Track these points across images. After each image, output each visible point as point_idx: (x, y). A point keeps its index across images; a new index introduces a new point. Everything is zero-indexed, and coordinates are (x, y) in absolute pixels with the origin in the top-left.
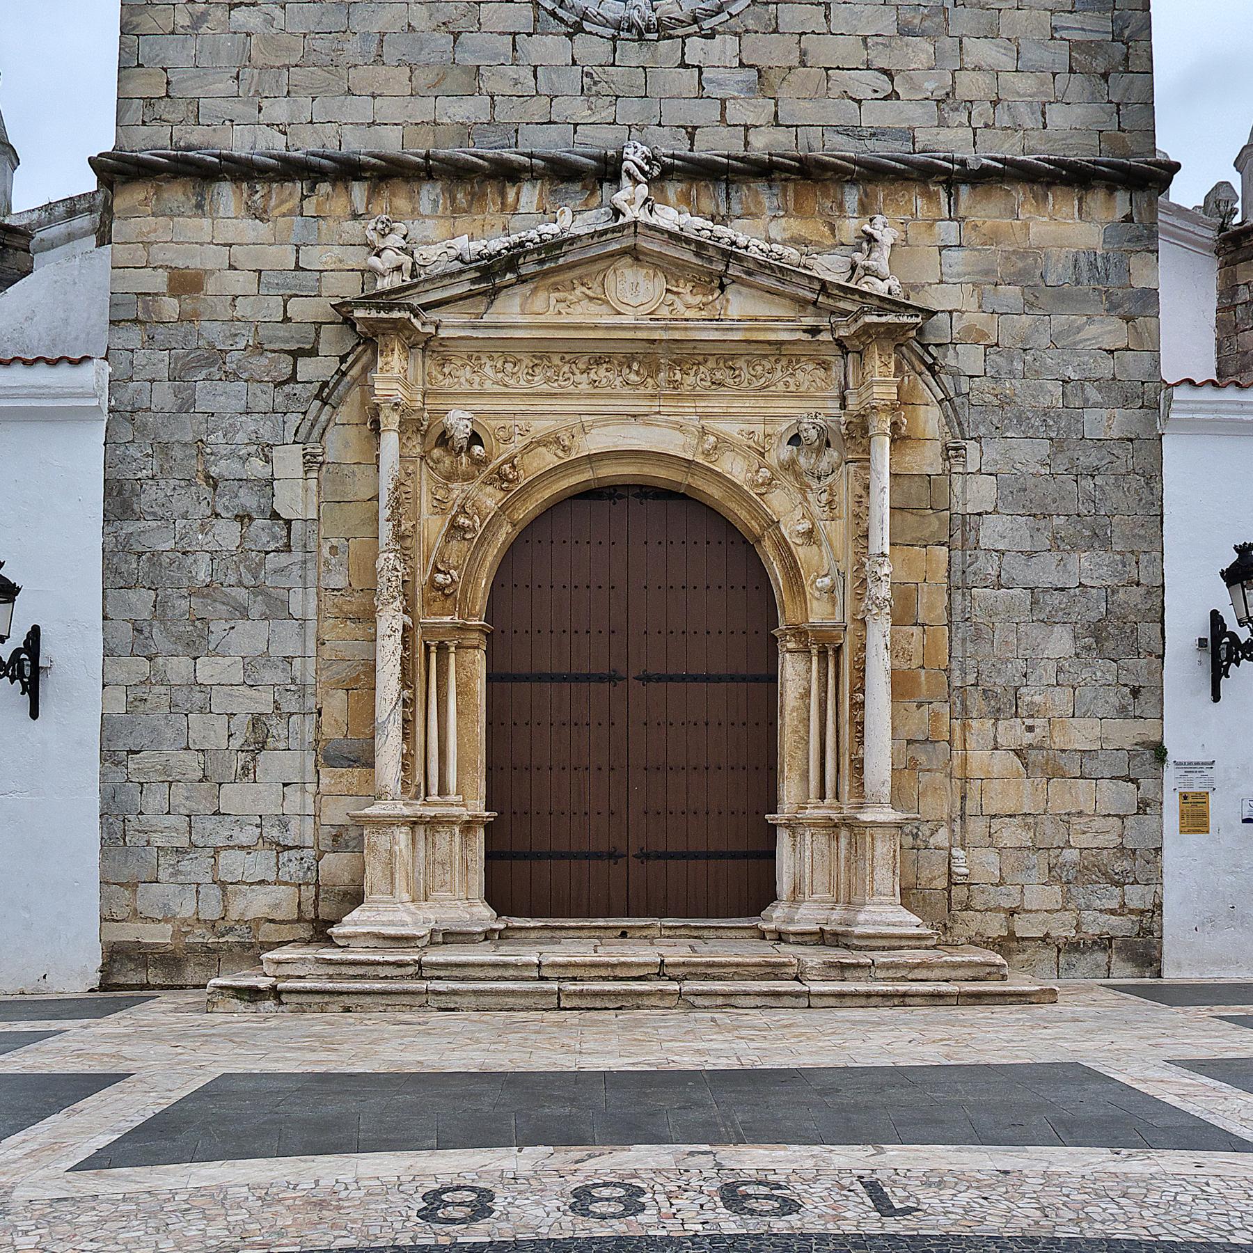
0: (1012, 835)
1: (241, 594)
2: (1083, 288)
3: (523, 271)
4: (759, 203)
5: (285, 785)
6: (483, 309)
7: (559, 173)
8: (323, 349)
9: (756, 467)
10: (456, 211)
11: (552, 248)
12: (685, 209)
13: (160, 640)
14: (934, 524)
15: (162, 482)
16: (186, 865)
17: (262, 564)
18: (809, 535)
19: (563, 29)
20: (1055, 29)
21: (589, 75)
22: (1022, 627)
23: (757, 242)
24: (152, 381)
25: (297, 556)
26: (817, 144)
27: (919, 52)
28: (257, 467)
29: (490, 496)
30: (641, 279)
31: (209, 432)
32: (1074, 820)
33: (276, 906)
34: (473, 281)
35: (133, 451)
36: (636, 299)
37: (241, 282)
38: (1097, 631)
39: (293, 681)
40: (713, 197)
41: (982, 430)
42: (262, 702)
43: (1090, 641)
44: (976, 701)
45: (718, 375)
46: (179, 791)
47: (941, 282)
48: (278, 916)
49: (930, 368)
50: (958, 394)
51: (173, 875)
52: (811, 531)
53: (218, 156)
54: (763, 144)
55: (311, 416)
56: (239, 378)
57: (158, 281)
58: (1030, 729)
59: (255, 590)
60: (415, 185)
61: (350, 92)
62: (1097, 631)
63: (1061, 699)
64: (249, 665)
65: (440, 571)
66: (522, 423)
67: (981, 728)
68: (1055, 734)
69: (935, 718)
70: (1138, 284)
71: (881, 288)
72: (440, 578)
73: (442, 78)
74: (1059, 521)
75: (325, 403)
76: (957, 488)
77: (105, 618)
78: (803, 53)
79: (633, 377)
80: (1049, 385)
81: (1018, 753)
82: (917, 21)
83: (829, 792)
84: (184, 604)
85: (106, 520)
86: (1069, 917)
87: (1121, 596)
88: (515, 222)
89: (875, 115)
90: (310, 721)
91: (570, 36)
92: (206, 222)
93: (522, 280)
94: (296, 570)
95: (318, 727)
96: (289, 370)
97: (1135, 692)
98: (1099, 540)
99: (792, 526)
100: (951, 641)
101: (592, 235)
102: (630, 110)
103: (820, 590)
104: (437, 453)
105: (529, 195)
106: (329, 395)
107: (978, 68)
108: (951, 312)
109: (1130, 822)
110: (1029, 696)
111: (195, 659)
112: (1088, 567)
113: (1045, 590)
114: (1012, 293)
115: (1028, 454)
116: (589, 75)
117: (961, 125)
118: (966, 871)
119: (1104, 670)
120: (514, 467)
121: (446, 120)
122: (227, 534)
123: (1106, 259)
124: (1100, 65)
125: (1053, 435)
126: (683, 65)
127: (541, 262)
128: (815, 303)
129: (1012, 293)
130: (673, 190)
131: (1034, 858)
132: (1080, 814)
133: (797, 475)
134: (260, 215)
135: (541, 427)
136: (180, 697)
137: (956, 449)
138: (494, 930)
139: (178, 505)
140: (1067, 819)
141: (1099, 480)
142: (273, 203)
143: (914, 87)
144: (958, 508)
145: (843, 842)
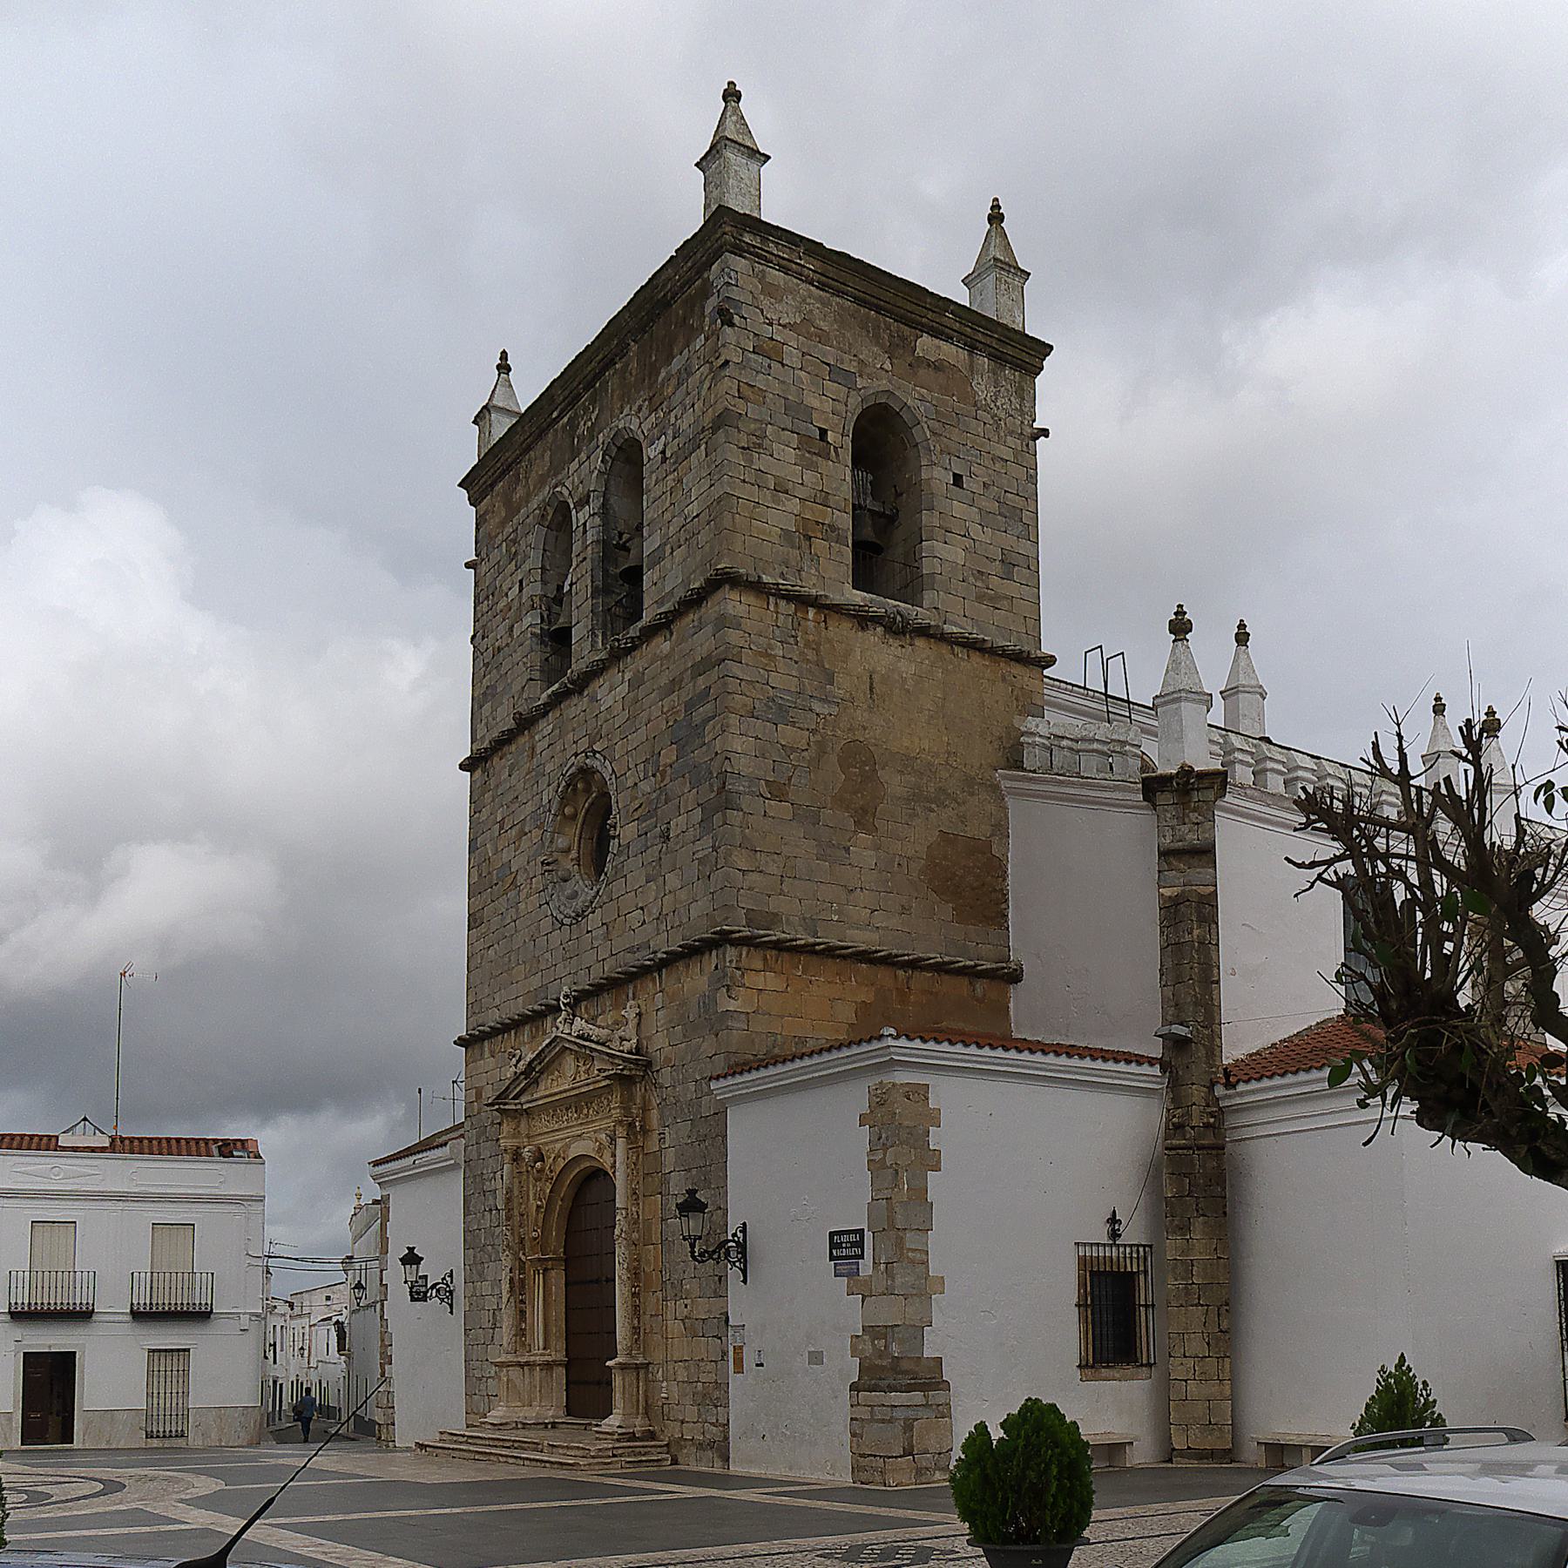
0: (682, 1375)
93: (541, 1072)
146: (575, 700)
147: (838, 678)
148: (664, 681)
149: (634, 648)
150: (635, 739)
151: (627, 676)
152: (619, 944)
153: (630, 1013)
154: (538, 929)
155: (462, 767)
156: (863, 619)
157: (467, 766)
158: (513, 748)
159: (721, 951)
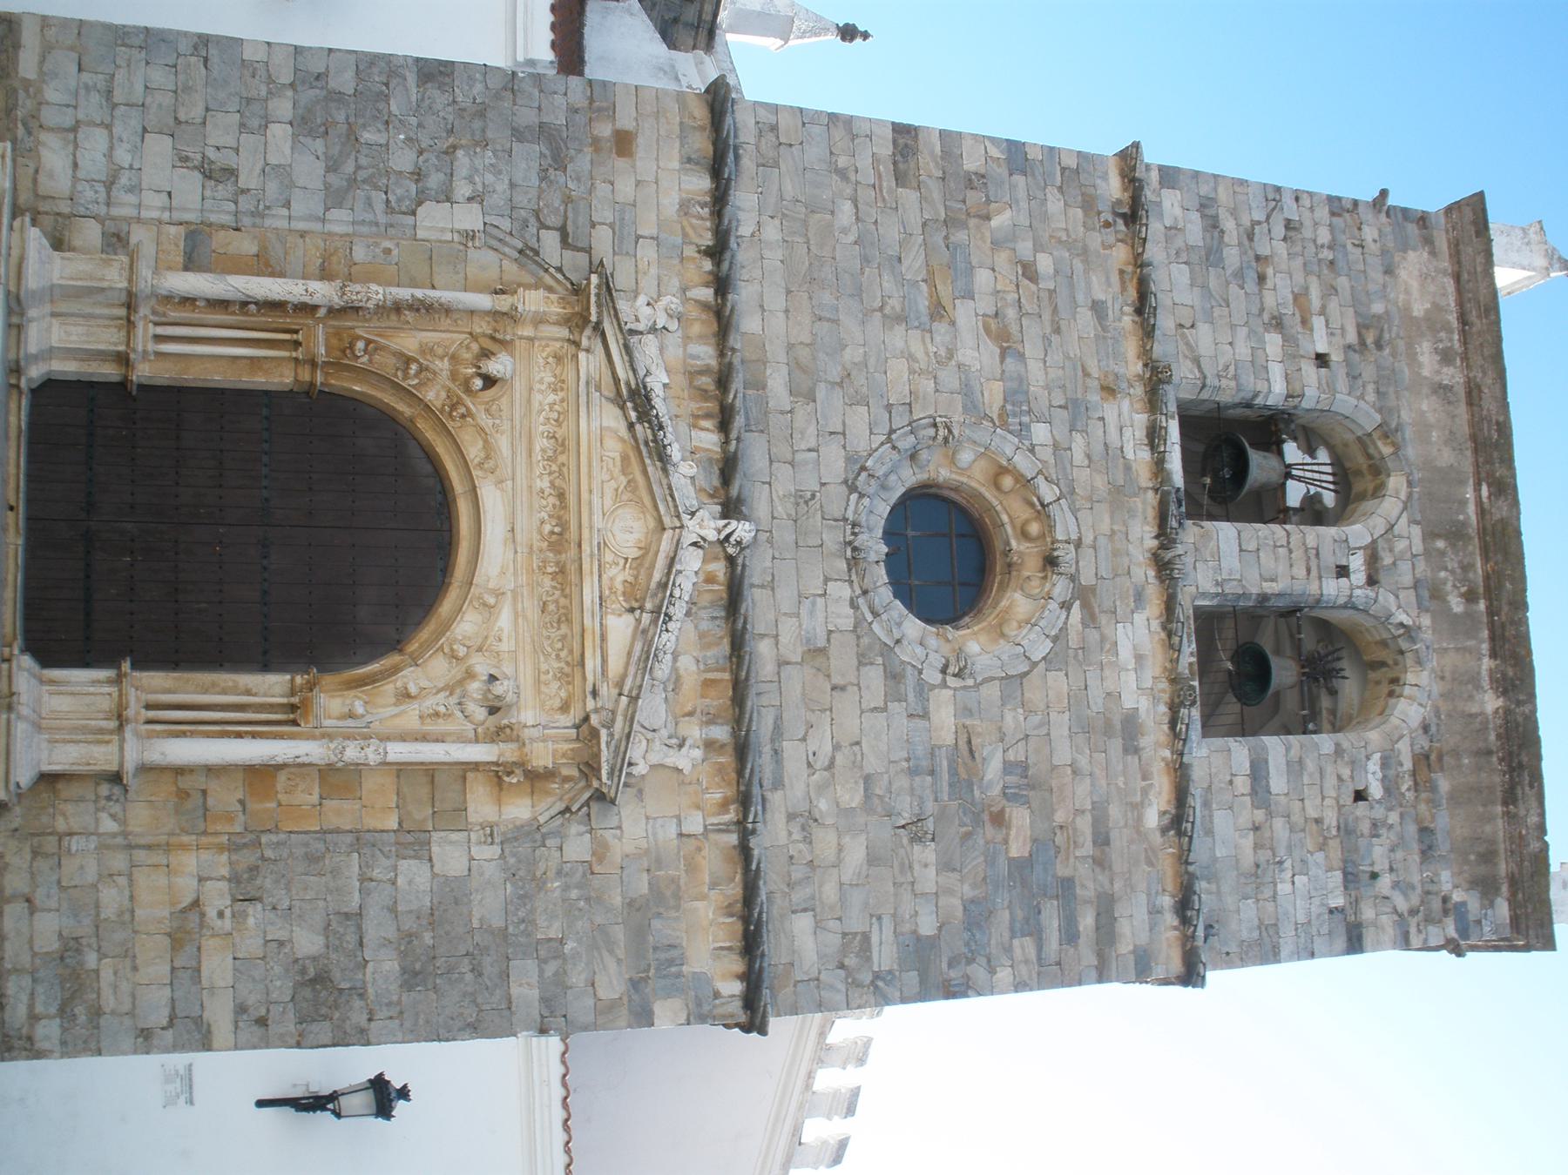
0: (111, 899)
1: (349, 167)
2: (651, 955)
3: (638, 427)
4: (707, 646)
5: (169, 194)
6: (606, 393)
7: (728, 467)
8: (568, 254)
9: (468, 643)
10: (692, 374)
11: (662, 457)
12: (702, 577)
13: (309, 95)
14: (422, 813)
15: (450, 109)
16: (95, 98)
17: (376, 188)
18: (406, 696)
19: (851, 476)
20: (879, 918)
21: (813, 496)
22: (321, 904)
23: (673, 639)
24: (539, 108)
25: (382, 219)
26: (764, 700)
27: (851, 796)
28: (462, 190)
29: (438, 395)
30: (636, 536)
31: (494, 152)
32: (128, 962)
33: (51, 176)
34: (628, 384)
35: (479, 87)
36: (619, 530)
37: (625, 189)
38: (321, 980)
39: (268, 208)
40: (713, 604)
41: (512, 861)
42: (248, 179)
43: (312, 972)
44: (247, 858)
45: (552, 607)
46: (168, 100)
47: (647, 818)
48: (42, 178)
49: (568, 809)
50: (544, 837)
51: (87, 88)
52: (408, 696)
53: (729, 180)
54: (763, 651)
55: (508, 239)
56: (542, 180)
57: (625, 121)
58: (221, 915)
59: (352, 182)
60: (713, 341)
61: (789, 292)
62: (321, 980)
63: (251, 945)
64: (283, 172)
65: (367, 346)
66: (506, 426)
67: (221, 864)
68: (217, 940)
69: (230, 818)
71: (636, 752)
72: (360, 345)
73: (804, 370)
74: (428, 938)
75: (521, 252)
76: (454, 836)
77: (330, 50)
78: (843, 688)
79: (547, 528)
80: (557, 925)
81: (196, 903)
82: (878, 791)
83: (152, 714)
84: (341, 117)
85: (418, 60)
86: (25, 960)
87: (357, 1003)
88: (683, 427)
89: (793, 752)
90: (227, 219)
91: (845, 482)
92: (676, 165)
93: (631, 426)
94: (369, 217)
95: (223, 227)
96: (549, 223)
97: (262, 1022)
98: (412, 978)
99: (411, 678)
100: (306, 833)
101: (670, 488)
102: (785, 535)
103: (352, 704)
104: (475, 347)
105: (709, 439)
106: (527, 256)
107: (840, 849)
108: (620, 828)
109: (127, 1021)
110: (254, 913)
111: (291, 123)
112: (384, 968)
113: (359, 927)
114: (642, 886)
115: (488, 907)
116: (813, 496)
117: (790, 834)
118: (74, 848)
119: (282, 988)
120: (463, 416)
121: (769, 372)
122: (403, 160)
123: (679, 975)
124: (851, 961)
125: (511, 929)
126: (827, 580)
127: (646, 444)
128: (620, 694)
129: (642, 886)
130: (719, 568)
131: (87, 921)
132: (135, 969)
133: (461, 682)
134: (684, 207)
135: (503, 443)
136: (256, 107)
137: (491, 835)
138: (19, 379)
139: (430, 121)
140: (128, 954)
141: (469, 977)
142: (694, 221)
143: (822, 788)
144: (435, 836)
145: (104, 724)
148: (1115, 812)
149: (1173, 723)
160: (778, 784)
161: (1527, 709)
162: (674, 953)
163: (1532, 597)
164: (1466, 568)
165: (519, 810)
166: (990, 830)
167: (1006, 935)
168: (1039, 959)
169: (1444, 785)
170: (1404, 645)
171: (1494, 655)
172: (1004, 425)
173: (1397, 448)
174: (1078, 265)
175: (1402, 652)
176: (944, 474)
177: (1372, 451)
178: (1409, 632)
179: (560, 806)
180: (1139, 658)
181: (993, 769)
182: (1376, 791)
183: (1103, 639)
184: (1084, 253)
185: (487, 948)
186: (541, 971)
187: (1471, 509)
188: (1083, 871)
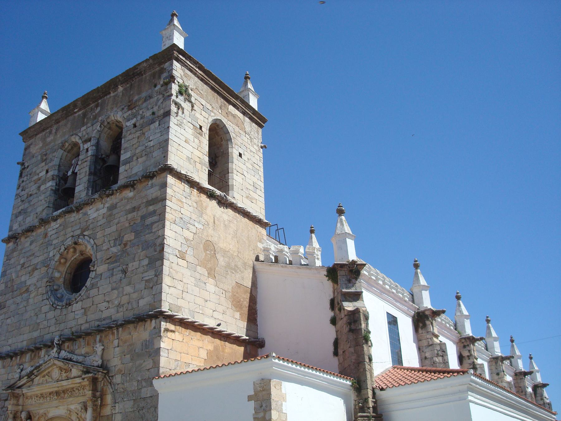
40: (73, 345)
41: (119, 399)
70: (156, 347)
78: (93, 302)
79: (56, 397)
105: (43, 352)
123: (149, 341)
125: (134, 398)
146: (74, 214)
147: (204, 216)
148: (128, 207)
150: (108, 231)
151: (107, 205)
152: (91, 317)
153: (99, 348)
154: (40, 311)
155: (3, 241)
156: (211, 196)
157: (7, 241)
158: (34, 234)
159: (158, 320)
160: (110, 317)
161: (120, 77)
162: (144, 344)
163: (95, 87)
164: (92, 109)
165: (109, 398)
166: (128, 247)
167: (152, 234)
168: (158, 222)
169: (136, 98)
170: (106, 123)
171: (110, 93)
172: (48, 265)
173: (66, 141)
174: (24, 251)
175: (108, 123)
176: (62, 280)
177: (70, 148)
178: (102, 123)
179: (109, 385)
180: (97, 210)
181: (114, 250)
182: (134, 121)
183: (92, 223)
184: (21, 250)
185: (138, 405)
186: (145, 387)
187: (80, 112)
188: (140, 213)
